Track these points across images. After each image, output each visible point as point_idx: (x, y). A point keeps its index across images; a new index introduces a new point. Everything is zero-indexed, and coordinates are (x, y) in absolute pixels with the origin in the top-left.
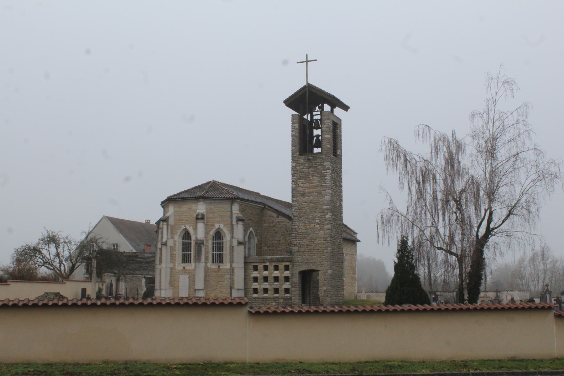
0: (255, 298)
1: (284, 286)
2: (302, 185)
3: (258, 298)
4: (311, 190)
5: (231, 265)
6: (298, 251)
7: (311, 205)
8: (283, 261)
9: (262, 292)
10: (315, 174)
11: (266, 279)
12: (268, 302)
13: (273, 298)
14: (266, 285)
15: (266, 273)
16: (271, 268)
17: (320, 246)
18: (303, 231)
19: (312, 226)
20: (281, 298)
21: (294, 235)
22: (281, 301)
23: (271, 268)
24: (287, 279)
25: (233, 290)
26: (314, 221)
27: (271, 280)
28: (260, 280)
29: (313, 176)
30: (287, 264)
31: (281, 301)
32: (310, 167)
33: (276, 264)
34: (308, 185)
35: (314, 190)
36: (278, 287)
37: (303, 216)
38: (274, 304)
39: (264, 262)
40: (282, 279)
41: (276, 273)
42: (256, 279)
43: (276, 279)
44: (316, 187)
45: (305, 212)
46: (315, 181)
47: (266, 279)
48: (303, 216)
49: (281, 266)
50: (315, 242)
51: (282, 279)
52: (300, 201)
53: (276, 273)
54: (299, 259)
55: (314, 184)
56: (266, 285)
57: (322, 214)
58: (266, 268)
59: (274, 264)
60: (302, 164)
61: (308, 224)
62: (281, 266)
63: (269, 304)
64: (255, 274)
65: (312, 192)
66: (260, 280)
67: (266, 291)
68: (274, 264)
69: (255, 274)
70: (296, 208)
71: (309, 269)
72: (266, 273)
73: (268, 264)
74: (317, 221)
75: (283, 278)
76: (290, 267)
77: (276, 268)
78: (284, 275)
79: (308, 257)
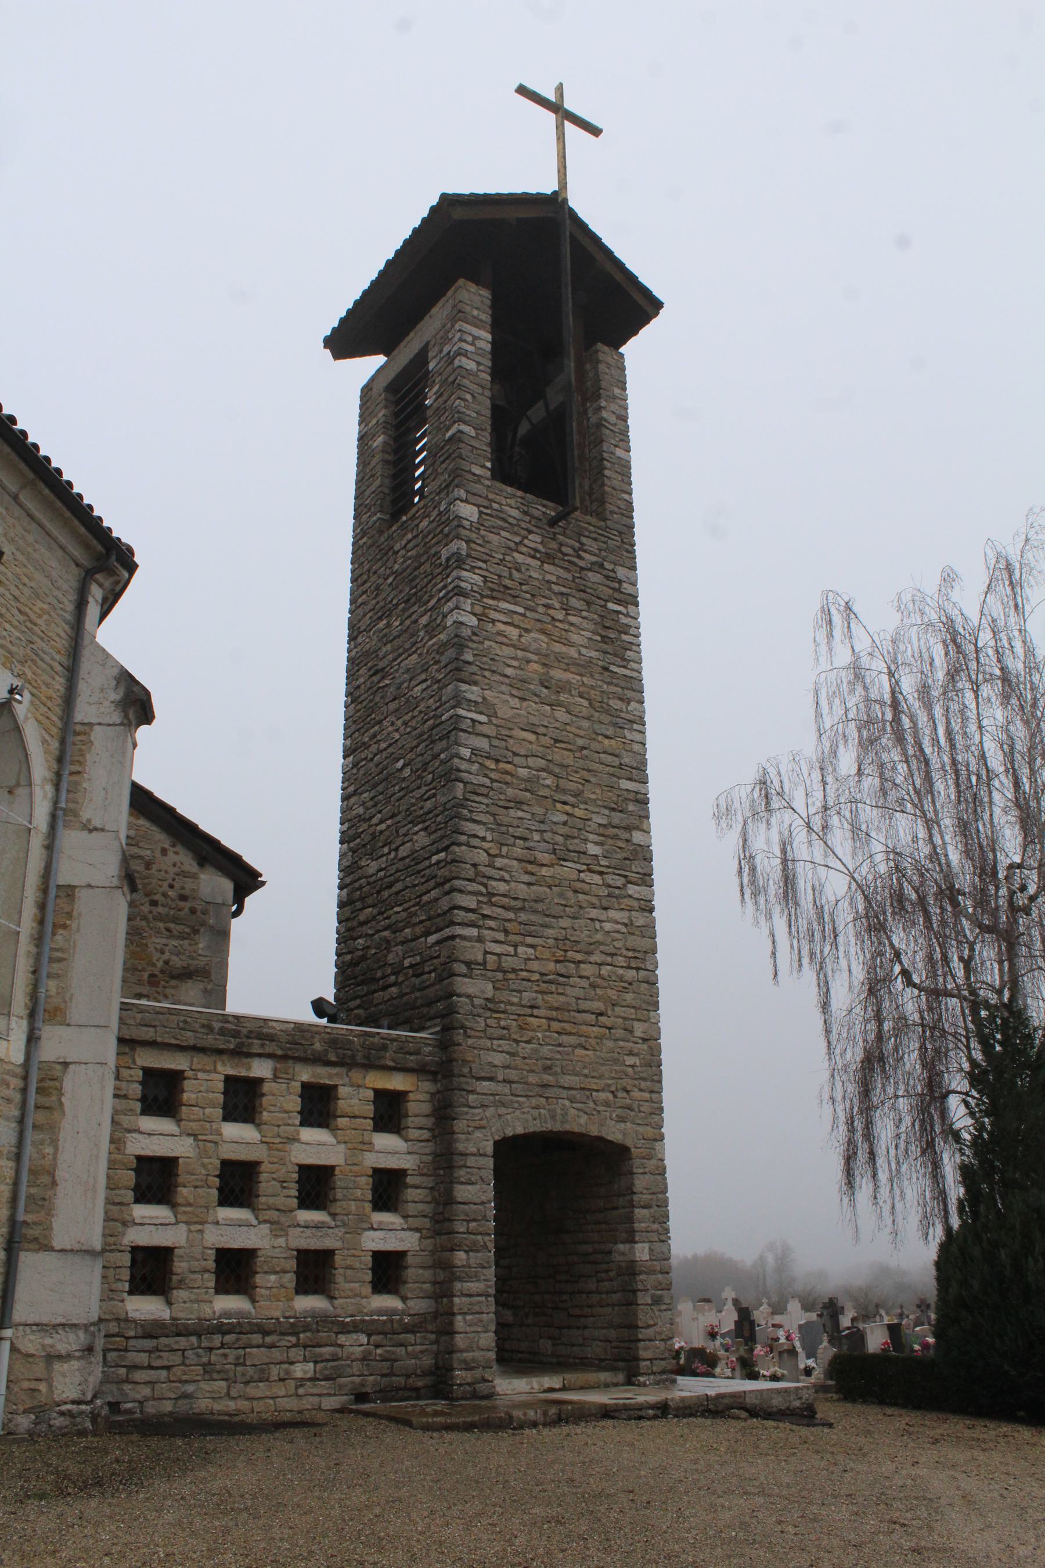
0: (152, 1330)
1: (374, 1241)
2: (513, 632)
3: (181, 1331)
4: (557, 674)
5: (32, 1039)
6: (491, 1006)
7: (559, 755)
8: (370, 1065)
9: (210, 1280)
10: (573, 602)
11: (238, 1183)
12: (258, 1355)
13: (295, 1327)
14: (234, 1227)
15: (239, 1138)
16: (282, 1099)
17: (612, 994)
18: (522, 891)
19: (567, 871)
20: (355, 1328)
21: (470, 902)
22: (355, 1344)
23: (282, 1099)
24: (387, 1187)
25: (28, 1261)
26: (573, 844)
27: (276, 1188)
28: (197, 1186)
29: (567, 609)
30: (397, 1082)
31: (355, 1344)
32: (547, 558)
33: (322, 1075)
34: (535, 639)
35: (575, 679)
36: (328, 1243)
37: (519, 804)
38: (301, 1370)
39: (240, 1053)
40: (354, 1191)
41: (316, 1145)
42: (156, 1179)
43: (315, 1185)
44: (584, 667)
45: (530, 785)
46: (575, 638)
47: (238, 1183)
48: (519, 804)
49: (355, 1095)
50: (587, 970)
51: (354, 1191)
52: (504, 712)
53: (316, 1145)
54: (498, 1059)
55: (573, 652)
56: (234, 1227)
57: (617, 818)
58: (242, 1100)
59: (306, 1074)
60: (511, 528)
61: (545, 858)
62: (355, 1095)
63: (264, 1378)
64: (158, 1137)
65: (563, 687)
66: (197, 1186)
67: (234, 1269)
68: (306, 1074)
69: (158, 1137)
70: (483, 744)
71: (558, 1127)
72: (239, 1138)
73: (261, 1069)
74: (593, 849)
75: (365, 1182)
76: (412, 1107)
77: (318, 1107)
78: (371, 1160)
79: (545, 1051)
